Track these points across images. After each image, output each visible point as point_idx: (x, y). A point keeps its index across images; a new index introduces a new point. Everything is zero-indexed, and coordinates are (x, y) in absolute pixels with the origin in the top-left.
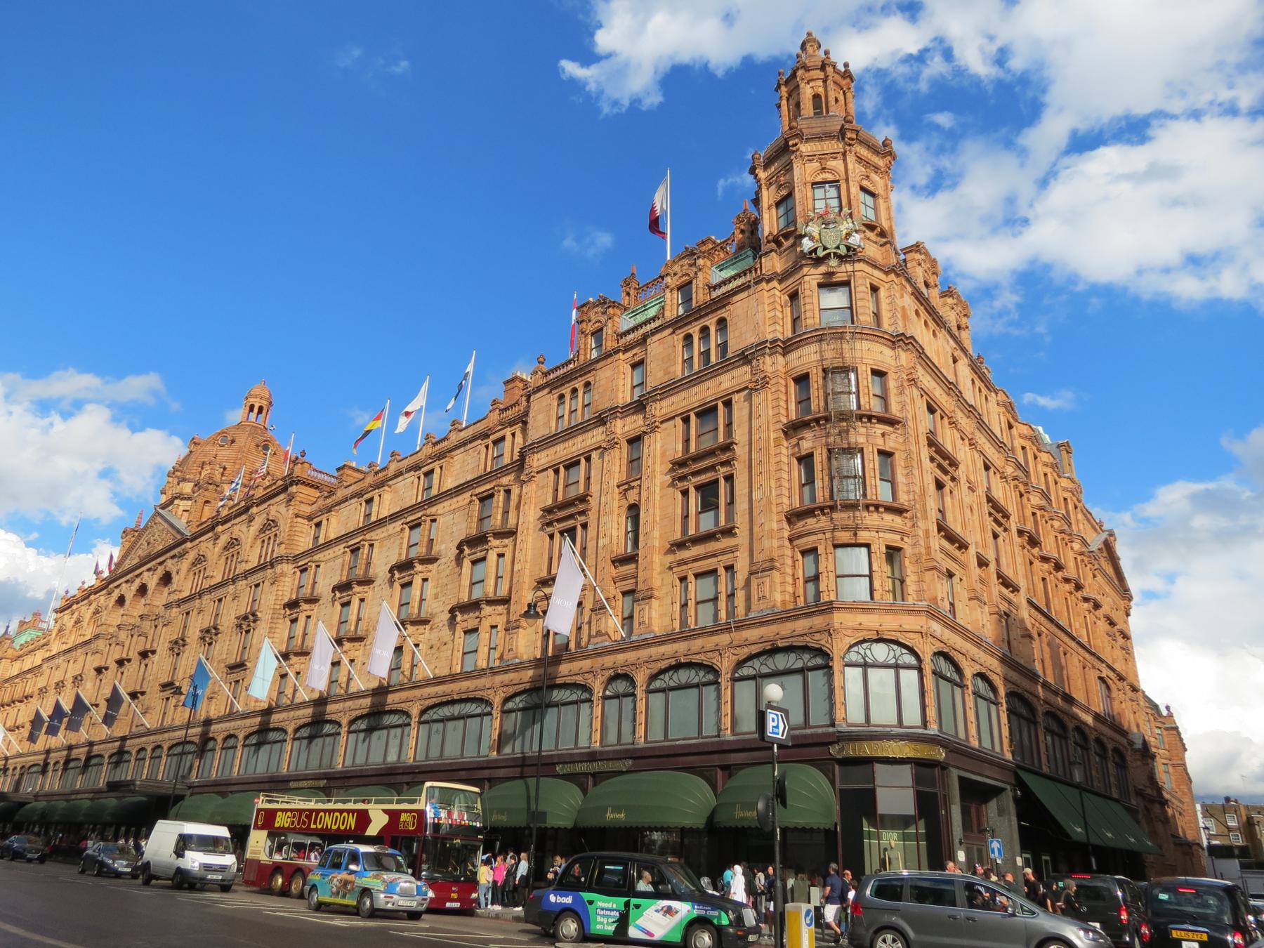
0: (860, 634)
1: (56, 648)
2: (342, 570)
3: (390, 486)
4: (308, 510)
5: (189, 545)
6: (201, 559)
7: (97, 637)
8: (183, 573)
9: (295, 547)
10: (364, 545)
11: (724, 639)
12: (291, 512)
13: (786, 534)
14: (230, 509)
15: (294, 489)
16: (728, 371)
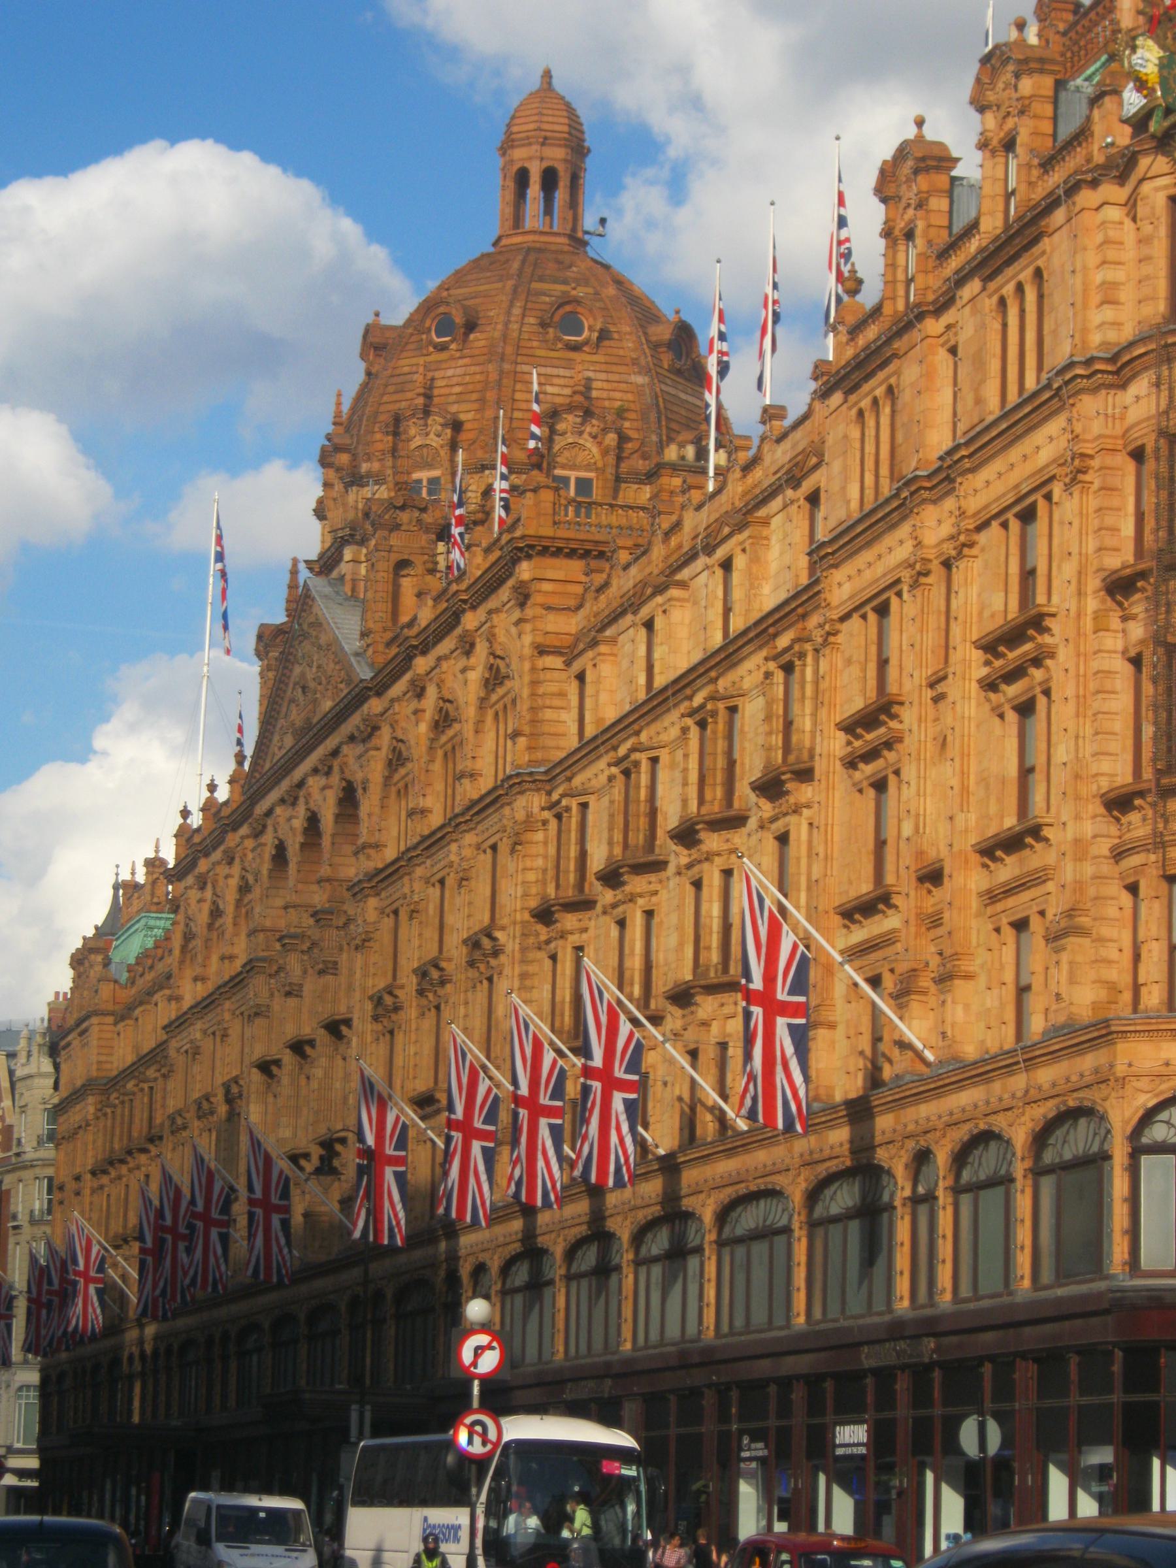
0: (1164, 1087)
1: (190, 992)
2: (611, 829)
3: (683, 585)
4: (570, 625)
5: (375, 705)
6: (397, 760)
7: (251, 967)
8: (375, 790)
9: (550, 742)
10: (637, 764)
11: (1019, 1082)
12: (527, 639)
13: (1103, 847)
14: (436, 599)
15: (525, 570)
16: (1019, 438)
